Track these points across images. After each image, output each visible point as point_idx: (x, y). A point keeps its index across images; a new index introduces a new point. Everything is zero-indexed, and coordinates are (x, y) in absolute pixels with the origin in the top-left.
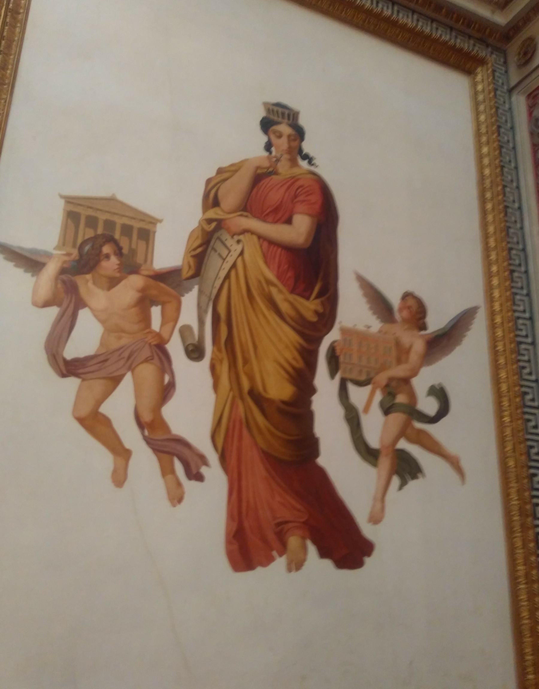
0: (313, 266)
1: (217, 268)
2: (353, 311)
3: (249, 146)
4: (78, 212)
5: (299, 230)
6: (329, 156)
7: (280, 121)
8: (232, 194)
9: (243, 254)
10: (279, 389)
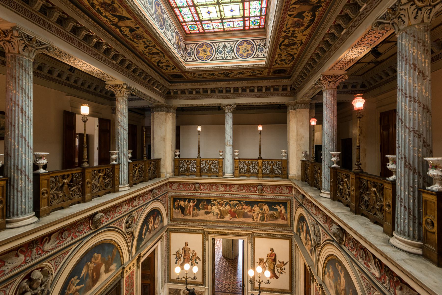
0: (275, 260)
1: (268, 261)
2: (278, 263)
3: (270, 252)
4: (259, 259)
5: (273, 257)
6: (276, 251)
7: (272, 250)
8: (268, 256)
9: (270, 260)
10: (272, 269)
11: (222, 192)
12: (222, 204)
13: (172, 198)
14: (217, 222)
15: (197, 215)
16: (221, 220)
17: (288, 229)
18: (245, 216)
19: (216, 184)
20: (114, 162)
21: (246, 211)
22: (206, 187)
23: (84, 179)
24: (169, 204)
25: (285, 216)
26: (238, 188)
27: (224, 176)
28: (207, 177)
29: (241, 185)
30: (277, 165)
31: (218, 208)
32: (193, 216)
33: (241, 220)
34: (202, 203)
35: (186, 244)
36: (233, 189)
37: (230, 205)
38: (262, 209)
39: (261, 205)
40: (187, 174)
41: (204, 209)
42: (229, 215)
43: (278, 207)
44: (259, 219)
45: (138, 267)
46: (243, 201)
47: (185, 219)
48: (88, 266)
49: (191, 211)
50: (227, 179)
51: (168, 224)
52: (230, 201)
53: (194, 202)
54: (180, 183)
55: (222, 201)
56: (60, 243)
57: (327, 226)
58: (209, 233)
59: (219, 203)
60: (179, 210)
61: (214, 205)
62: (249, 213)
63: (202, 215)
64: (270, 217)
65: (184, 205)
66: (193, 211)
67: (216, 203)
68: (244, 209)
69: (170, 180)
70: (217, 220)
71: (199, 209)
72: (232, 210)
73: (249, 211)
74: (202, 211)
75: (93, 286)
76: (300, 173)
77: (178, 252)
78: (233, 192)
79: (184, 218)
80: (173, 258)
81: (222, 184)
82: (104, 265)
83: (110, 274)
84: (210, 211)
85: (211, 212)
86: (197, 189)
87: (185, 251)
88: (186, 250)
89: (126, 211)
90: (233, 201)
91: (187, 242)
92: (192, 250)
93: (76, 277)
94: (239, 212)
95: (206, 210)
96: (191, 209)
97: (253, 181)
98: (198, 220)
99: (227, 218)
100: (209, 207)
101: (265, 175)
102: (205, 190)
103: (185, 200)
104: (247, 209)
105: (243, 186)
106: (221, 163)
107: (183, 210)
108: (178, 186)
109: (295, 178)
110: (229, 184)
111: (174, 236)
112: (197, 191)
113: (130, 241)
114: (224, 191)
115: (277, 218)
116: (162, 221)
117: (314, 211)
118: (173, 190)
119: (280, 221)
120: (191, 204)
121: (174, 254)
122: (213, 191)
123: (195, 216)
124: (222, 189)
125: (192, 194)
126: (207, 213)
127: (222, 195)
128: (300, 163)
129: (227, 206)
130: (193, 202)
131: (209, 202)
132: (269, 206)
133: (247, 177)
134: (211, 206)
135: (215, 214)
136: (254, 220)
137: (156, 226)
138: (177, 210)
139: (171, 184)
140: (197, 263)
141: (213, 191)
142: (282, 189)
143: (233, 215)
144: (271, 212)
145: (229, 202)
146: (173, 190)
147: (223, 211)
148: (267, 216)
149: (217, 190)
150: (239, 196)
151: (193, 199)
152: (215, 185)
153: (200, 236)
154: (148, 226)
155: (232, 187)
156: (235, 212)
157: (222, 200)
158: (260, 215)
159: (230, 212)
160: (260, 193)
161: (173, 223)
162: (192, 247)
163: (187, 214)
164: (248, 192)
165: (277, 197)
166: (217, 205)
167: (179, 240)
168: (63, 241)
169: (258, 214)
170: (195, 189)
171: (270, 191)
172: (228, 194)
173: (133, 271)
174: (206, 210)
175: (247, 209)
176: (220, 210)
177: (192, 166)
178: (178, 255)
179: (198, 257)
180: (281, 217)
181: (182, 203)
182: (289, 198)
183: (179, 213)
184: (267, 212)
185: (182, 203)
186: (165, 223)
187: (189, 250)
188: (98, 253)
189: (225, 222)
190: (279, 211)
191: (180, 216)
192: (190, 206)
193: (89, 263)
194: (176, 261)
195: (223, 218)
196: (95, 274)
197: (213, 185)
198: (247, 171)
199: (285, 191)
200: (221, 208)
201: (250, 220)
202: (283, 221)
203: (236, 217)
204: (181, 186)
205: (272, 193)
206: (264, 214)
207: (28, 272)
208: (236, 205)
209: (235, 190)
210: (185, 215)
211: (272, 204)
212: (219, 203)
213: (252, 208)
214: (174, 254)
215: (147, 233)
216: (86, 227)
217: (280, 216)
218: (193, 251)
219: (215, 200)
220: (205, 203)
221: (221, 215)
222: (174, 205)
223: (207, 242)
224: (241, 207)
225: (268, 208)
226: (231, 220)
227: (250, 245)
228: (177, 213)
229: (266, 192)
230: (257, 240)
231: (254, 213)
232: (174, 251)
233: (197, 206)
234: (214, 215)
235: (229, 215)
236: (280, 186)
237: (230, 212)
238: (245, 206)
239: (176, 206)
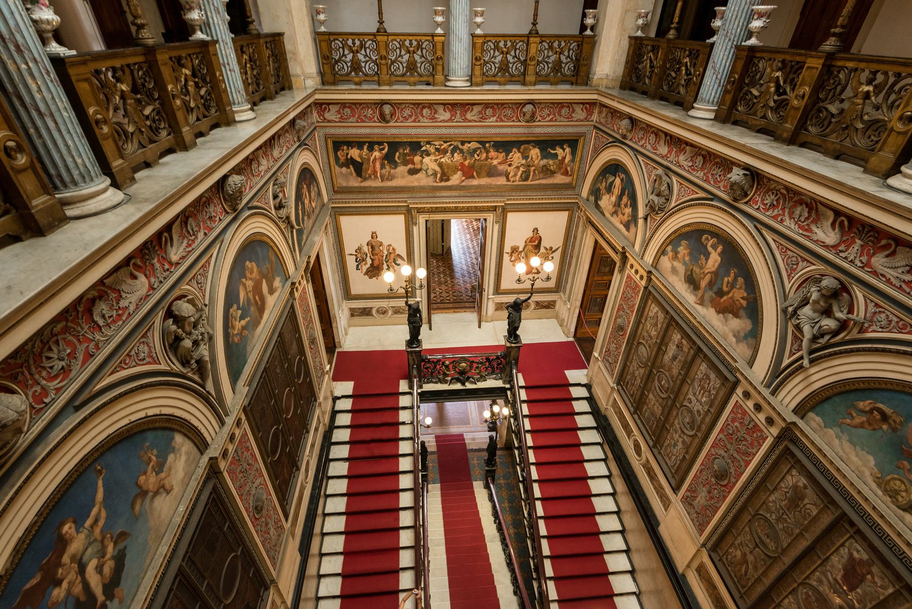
3: (531, 235)
7: (536, 230)
11: (444, 124)
12: (445, 152)
13: (330, 142)
14: (435, 189)
15: (391, 178)
16: (443, 184)
17: (570, 192)
18: (492, 172)
19: (431, 105)
20: (199, 35)
21: (495, 162)
22: (407, 112)
23: (160, 85)
24: (325, 155)
25: (569, 169)
26: (480, 112)
27: (448, 84)
28: (408, 87)
29: (487, 105)
30: (569, 50)
31: (436, 160)
33: (484, 181)
34: (400, 151)
36: (469, 116)
37: (462, 151)
38: (526, 157)
39: (525, 149)
40: (357, 79)
41: (405, 163)
42: (459, 173)
43: (559, 151)
44: (518, 178)
45: (308, 281)
46: (489, 142)
47: (365, 187)
48: (244, 285)
49: (378, 170)
50: (455, 90)
51: (330, 200)
52: (463, 143)
53: (383, 149)
54: (343, 104)
55: (445, 145)
56: (190, 245)
57: (701, 174)
58: (420, 211)
59: (437, 150)
60: (349, 168)
61: (428, 154)
62: (501, 167)
63: (403, 177)
64: (540, 173)
65: (360, 156)
66: (381, 169)
67: (432, 150)
68: (492, 159)
69: (317, 96)
70: (435, 184)
71: (395, 165)
72: (466, 163)
73: (500, 163)
74: (402, 169)
75: (261, 317)
76: (620, 70)
78: (470, 121)
79: (362, 185)
80: (351, 262)
81: (447, 105)
82: (264, 281)
83: (276, 294)
84: (419, 167)
86: (388, 117)
88: (374, 246)
89: (266, 171)
90: (469, 142)
91: (374, 230)
92: (385, 244)
93: (235, 306)
94: (481, 167)
95: (410, 166)
96: (378, 165)
97: (514, 93)
98: (395, 187)
99: (456, 179)
100: (417, 159)
101: (542, 79)
102: (406, 119)
103: (360, 145)
104: (497, 158)
105: (492, 107)
106: (439, 47)
107: (359, 168)
108: (338, 112)
109: (605, 82)
110: (461, 104)
111: (345, 221)
112: (388, 122)
113: (289, 235)
114: (450, 120)
115: (553, 173)
116: (319, 194)
117: (663, 149)
118: (329, 121)
119: (559, 179)
120: (377, 154)
122: (425, 122)
123: (387, 179)
124: (443, 115)
125: (376, 131)
126: (413, 172)
127: (444, 131)
128: (625, 43)
129: (456, 155)
131: (415, 147)
132: (542, 150)
133: (500, 84)
135: (430, 172)
136: (508, 180)
137: (314, 205)
139: (321, 106)
140: (398, 265)
141: (425, 122)
142: (574, 111)
143: (468, 173)
144: (544, 162)
145: (460, 146)
146: (329, 121)
147: (448, 165)
148: (534, 171)
149: (433, 119)
150: (481, 131)
151: (380, 143)
152: (429, 107)
153: (402, 217)
154: (303, 203)
155: (466, 112)
156: (472, 167)
157: (445, 142)
158: (521, 169)
159: (462, 168)
160: (528, 122)
161: (339, 196)
162: (385, 239)
163: (370, 177)
164: (502, 121)
165: (560, 130)
166: (434, 153)
167: (357, 230)
168: (193, 241)
169: (518, 168)
170: (383, 118)
171: (549, 115)
172: (459, 127)
173: (304, 288)
174: (410, 166)
175: (496, 158)
176: (440, 165)
177: (366, 56)
180: (562, 170)
181: (354, 153)
182: (583, 130)
184: (536, 162)
185: (354, 153)
186: (326, 199)
187: (381, 244)
188: (250, 262)
189: (450, 188)
190: (560, 158)
191: (355, 182)
192: (375, 159)
193: (244, 280)
194: (357, 266)
195: (448, 180)
196: (257, 298)
197: (424, 107)
198: (500, 69)
199: (580, 114)
200: (443, 160)
201: (502, 181)
202: (564, 177)
203: (474, 177)
204: (348, 111)
205: (551, 120)
206: (529, 166)
207: (165, 304)
208: (475, 151)
209: (474, 118)
210: (365, 179)
211: (546, 145)
212: (437, 150)
213: (507, 155)
215: (306, 218)
216: (219, 209)
217: (560, 169)
218: (390, 245)
219: (428, 143)
220: (407, 151)
221: (443, 174)
222: (337, 159)
223: (415, 229)
224: (484, 155)
225: (539, 154)
226: (463, 184)
227: (496, 227)
228: (346, 176)
229: (539, 118)
230: (510, 216)
231: (510, 165)
233: (389, 158)
234: (428, 176)
235: (459, 173)
236: (570, 104)
237: (462, 168)
238: (493, 153)
239: (342, 159)
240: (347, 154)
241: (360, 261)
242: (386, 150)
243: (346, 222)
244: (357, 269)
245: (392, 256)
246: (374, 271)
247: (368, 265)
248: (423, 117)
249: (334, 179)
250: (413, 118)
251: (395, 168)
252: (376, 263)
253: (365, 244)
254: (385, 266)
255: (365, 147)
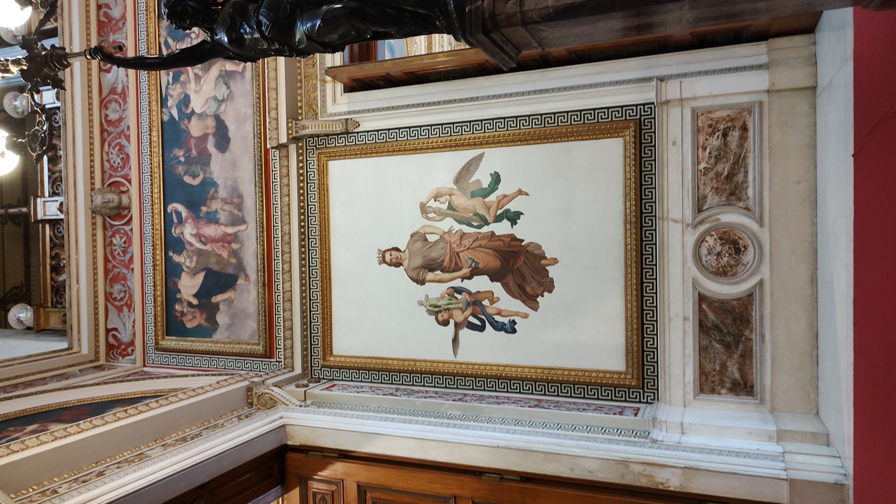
13: (171, 342)
15: (236, 199)
32: (243, 221)
35: (391, 258)
41: (204, 159)
53: (179, 214)
60: (216, 307)
61: (185, 101)
63: (234, 166)
65: (194, 273)
66: (217, 222)
71: (209, 184)
77: (440, 313)
79: (253, 276)
80: (483, 349)
84: (211, 122)
85: (217, 118)
87: (430, 266)
91: (375, 257)
95: (211, 146)
96: (211, 231)
100: (195, 128)
103: (172, 272)
107: (219, 281)
120: (188, 232)
121: (455, 341)
123: (240, 207)
126: (223, 139)
130: (181, 222)
131: (172, 133)
134: (189, 117)
135: (222, 91)
138: (222, 318)
140: (496, 179)
153: (336, 168)
166: (184, 84)
174: (211, 146)
178: (459, 316)
179: (458, 180)
183: (230, 302)
187: (419, 237)
194: (499, 327)
214: (455, 341)
218: (424, 209)
219: (163, 102)
220: (180, 153)
223: (368, 124)
232: (430, 344)
240: (190, 304)
241: (479, 316)
242: (180, 207)
243: (348, 341)
244: (511, 329)
245: (462, 201)
246: (523, 270)
247: (497, 288)
248: (120, 120)
249: (237, 348)
250: (124, 142)
251: (214, 184)
252: (487, 259)
253: (420, 291)
254: (502, 228)
255: (177, 258)
